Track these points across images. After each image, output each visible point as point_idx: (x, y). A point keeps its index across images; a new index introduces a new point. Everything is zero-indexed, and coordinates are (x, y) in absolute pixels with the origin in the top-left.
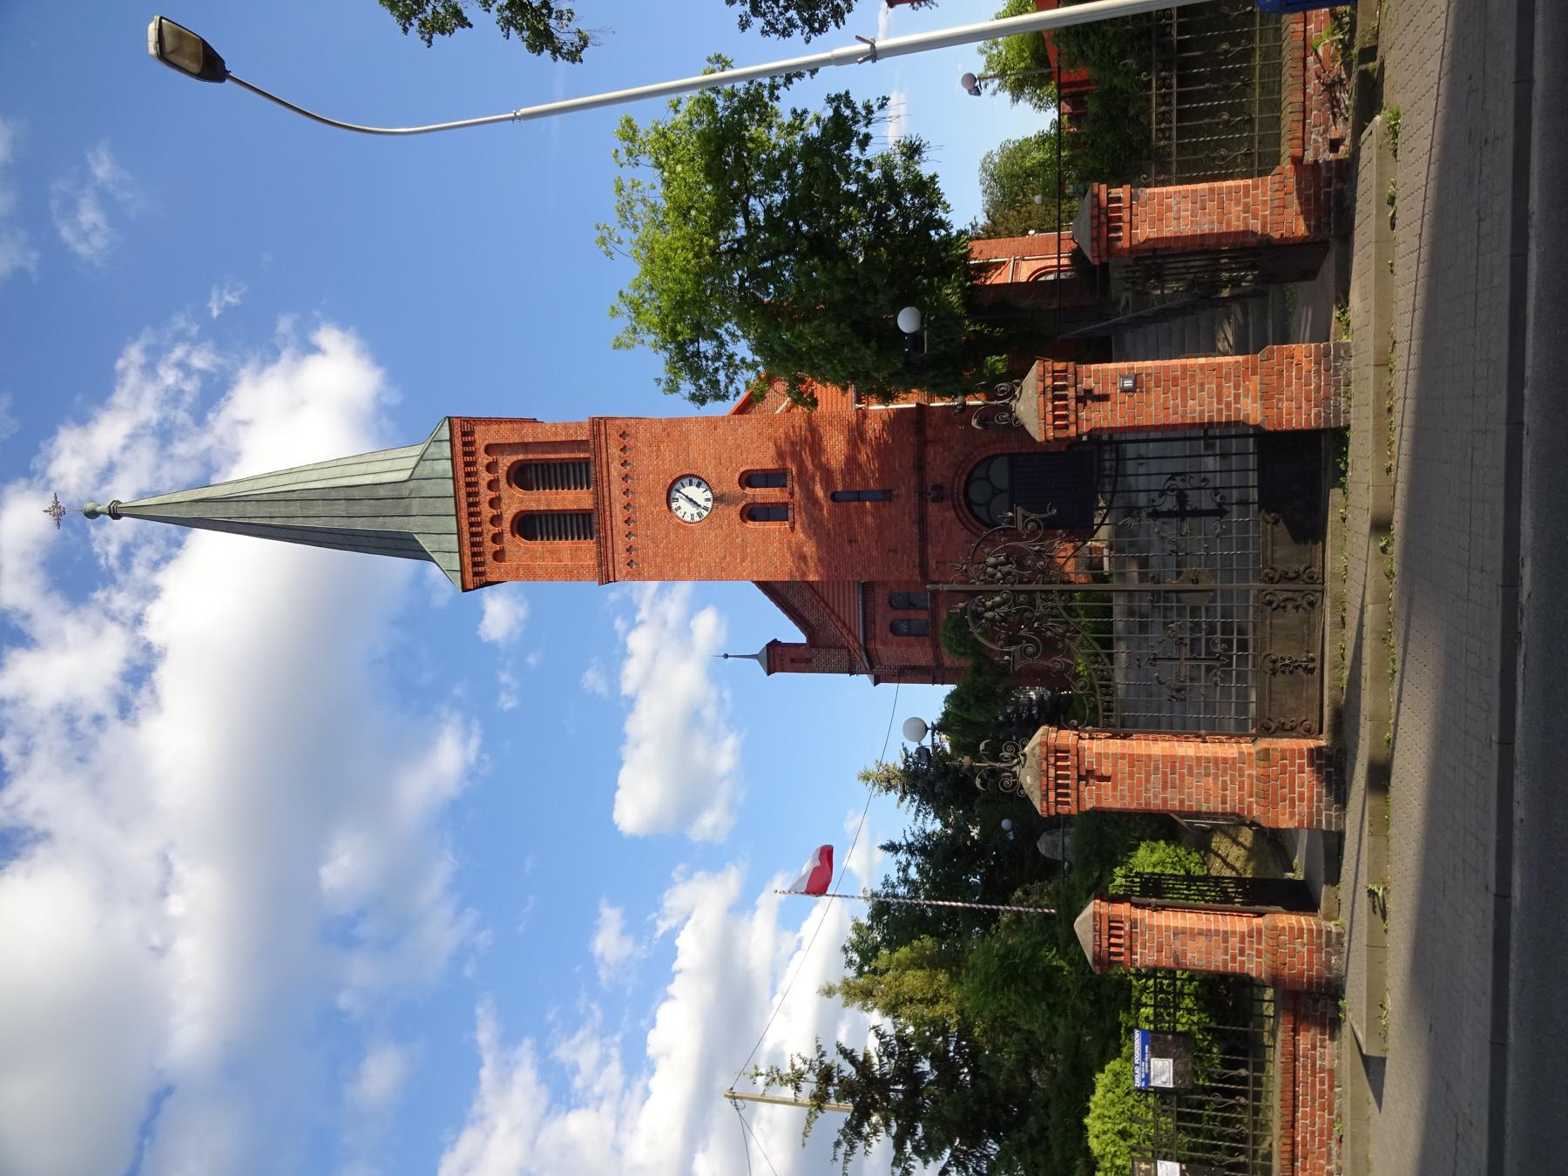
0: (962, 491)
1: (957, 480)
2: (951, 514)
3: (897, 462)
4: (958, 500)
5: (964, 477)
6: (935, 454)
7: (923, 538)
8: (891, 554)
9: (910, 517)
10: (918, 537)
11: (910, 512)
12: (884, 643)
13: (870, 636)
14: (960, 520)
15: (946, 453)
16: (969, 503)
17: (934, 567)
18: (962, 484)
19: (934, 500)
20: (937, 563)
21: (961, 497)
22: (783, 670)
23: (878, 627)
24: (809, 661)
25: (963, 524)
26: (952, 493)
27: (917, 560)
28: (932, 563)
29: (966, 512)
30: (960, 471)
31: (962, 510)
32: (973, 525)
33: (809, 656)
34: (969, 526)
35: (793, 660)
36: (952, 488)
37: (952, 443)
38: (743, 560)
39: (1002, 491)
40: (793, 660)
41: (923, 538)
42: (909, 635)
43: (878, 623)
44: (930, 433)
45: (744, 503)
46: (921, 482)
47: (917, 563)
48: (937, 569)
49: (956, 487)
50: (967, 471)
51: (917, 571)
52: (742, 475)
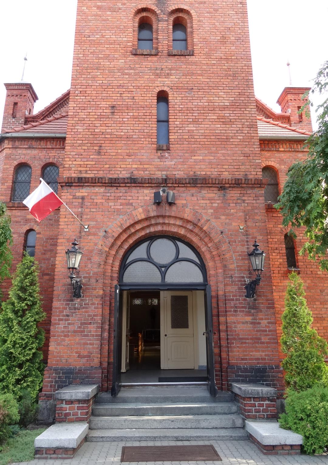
0: (166, 228)
1: (179, 223)
2: (140, 214)
3: (201, 158)
4: (157, 224)
5: (182, 232)
7: (114, 183)
10: (115, 176)
11: (145, 170)
12: (8, 157)
13: (17, 143)
14: (133, 225)
16: (151, 238)
17: (78, 194)
18: (174, 229)
19: (157, 195)
20: (83, 198)
21: (159, 228)
22: (8, 96)
23: (24, 152)
24: (14, 116)
25: (128, 228)
26: (164, 217)
27: (88, 176)
28: (83, 192)
29: (143, 233)
30: (190, 227)
31: (143, 229)
32: (126, 240)
33: (18, 116)
34: (125, 236)
35: (16, 104)
36: (170, 217)
37: (223, 217)
38: (99, 8)
39: (163, 275)
40: (16, 104)
41: (114, 183)
42: (14, 182)
43: (29, 151)
44: (234, 194)
45: (158, 12)
46: (179, 183)
47: (84, 175)
48: (75, 197)
49: (172, 221)
50: (189, 235)
51: (74, 175)
52: (187, 12)
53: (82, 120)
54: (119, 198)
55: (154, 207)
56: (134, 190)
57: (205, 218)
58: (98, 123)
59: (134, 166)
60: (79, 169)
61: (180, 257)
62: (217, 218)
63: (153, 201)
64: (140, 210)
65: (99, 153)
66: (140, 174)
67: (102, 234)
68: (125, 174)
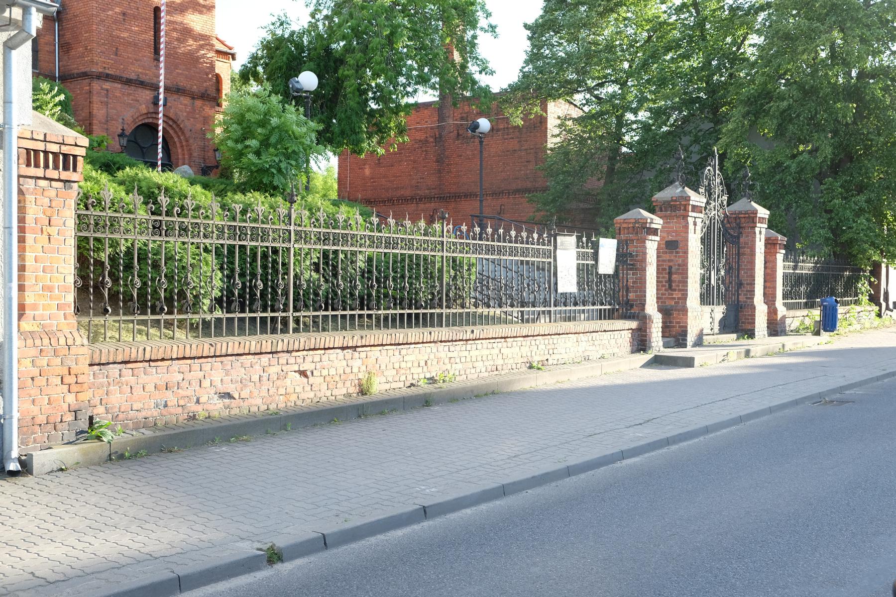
3: (181, 71)
6: (186, 105)
7: (128, 82)
8: (114, 49)
9: (141, 73)
11: (146, 75)
15: (185, 114)
20: (107, 90)
28: (107, 85)
37: (192, 120)
41: (128, 82)
44: (198, 103)
47: (107, 71)
48: (102, 89)
53: (102, 21)
54: (130, 94)
55: (152, 106)
56: (140, 90)
57: (182, 118)
58: (114, 27)
59: (140, 70)
60: (104, 65)
61: (133, 140)
62: (189, 120)
63: (152, 100)
64: (144, 106)
65: (116, 55)
66: (143, 78)
67: (120, 120)
68: (133, 76)
